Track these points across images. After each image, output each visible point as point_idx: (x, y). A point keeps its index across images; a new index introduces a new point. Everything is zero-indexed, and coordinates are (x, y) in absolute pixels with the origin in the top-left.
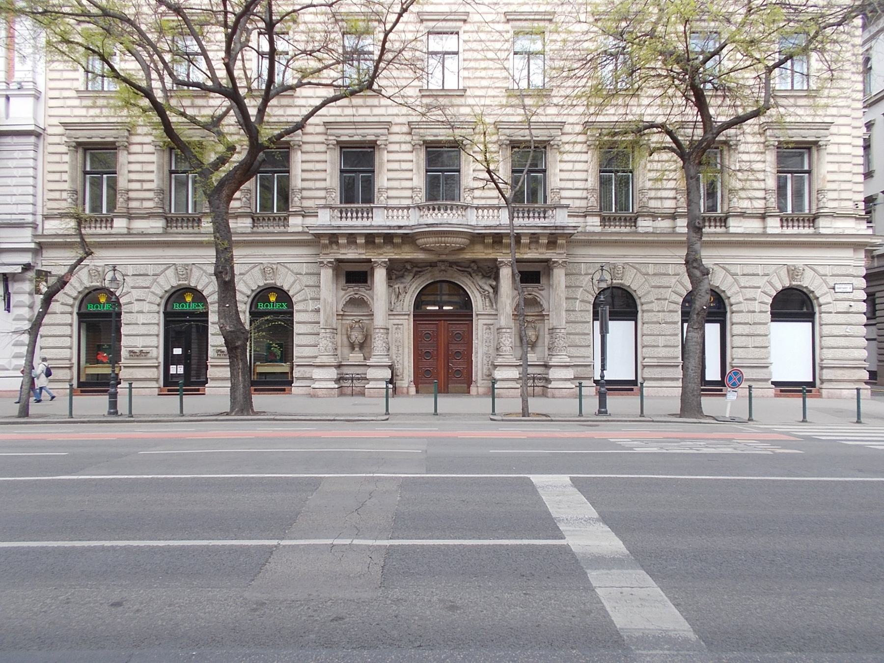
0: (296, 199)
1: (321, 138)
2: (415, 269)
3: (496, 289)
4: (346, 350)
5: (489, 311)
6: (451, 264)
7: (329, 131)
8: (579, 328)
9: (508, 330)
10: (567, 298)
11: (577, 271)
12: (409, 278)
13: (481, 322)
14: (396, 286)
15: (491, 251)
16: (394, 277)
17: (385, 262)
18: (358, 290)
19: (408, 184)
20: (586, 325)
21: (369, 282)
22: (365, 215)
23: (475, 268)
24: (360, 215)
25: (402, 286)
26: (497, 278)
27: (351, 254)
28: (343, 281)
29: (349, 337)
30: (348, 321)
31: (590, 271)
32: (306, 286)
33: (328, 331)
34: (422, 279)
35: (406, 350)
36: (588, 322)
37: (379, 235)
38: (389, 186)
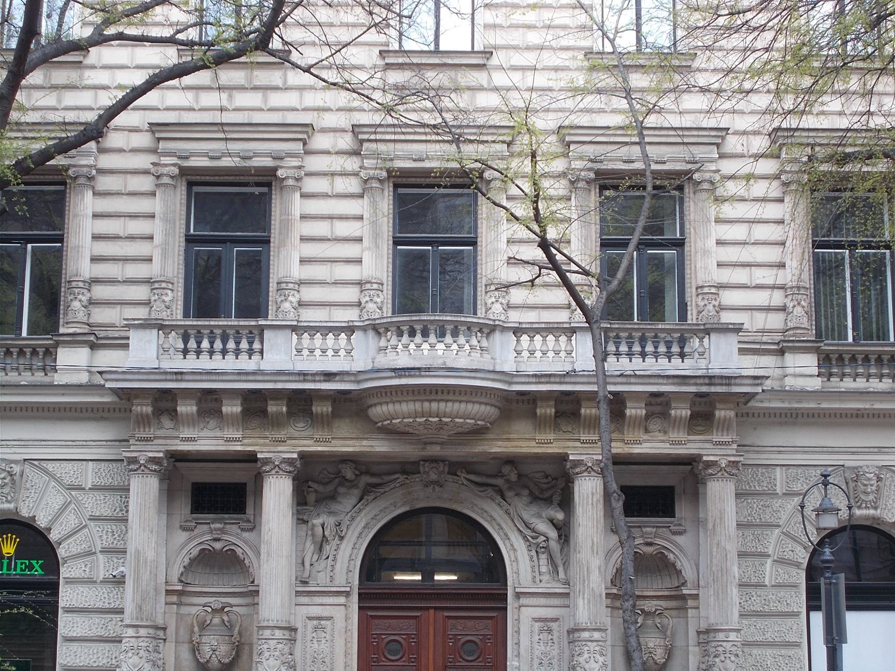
0: (76, 304)
1: (144, 161)
2: (366, 479)
3: (564, 531)
5: (548, 585)
6: (455, 467)
7: (162, 145)
8: (773, 630)
9: (597, 635)
10: (742, 555)
11: (764, 487)
12: (347, 503)
13: (528, 613)
14: (317, 521)
15: (551, 436)
16: (312, 498)
17: (290, 462)
18: (222, 531)
19: (351, 272)
20: (790, 622)
21: (250, 510)
22: (244, 345)
23: (513, 477)
24: (231, 345)
25: (330, 521)
26: (566, 502)
27: (207, 440)
28: (184, 508)
29: (195, 649)
30: (194, 609)
31: (798, 487)
32: (93, 519)
33: (143, 632)
34: (382, 503)
36: (796, 615)
37: (276, 395)
38: (304, 277)
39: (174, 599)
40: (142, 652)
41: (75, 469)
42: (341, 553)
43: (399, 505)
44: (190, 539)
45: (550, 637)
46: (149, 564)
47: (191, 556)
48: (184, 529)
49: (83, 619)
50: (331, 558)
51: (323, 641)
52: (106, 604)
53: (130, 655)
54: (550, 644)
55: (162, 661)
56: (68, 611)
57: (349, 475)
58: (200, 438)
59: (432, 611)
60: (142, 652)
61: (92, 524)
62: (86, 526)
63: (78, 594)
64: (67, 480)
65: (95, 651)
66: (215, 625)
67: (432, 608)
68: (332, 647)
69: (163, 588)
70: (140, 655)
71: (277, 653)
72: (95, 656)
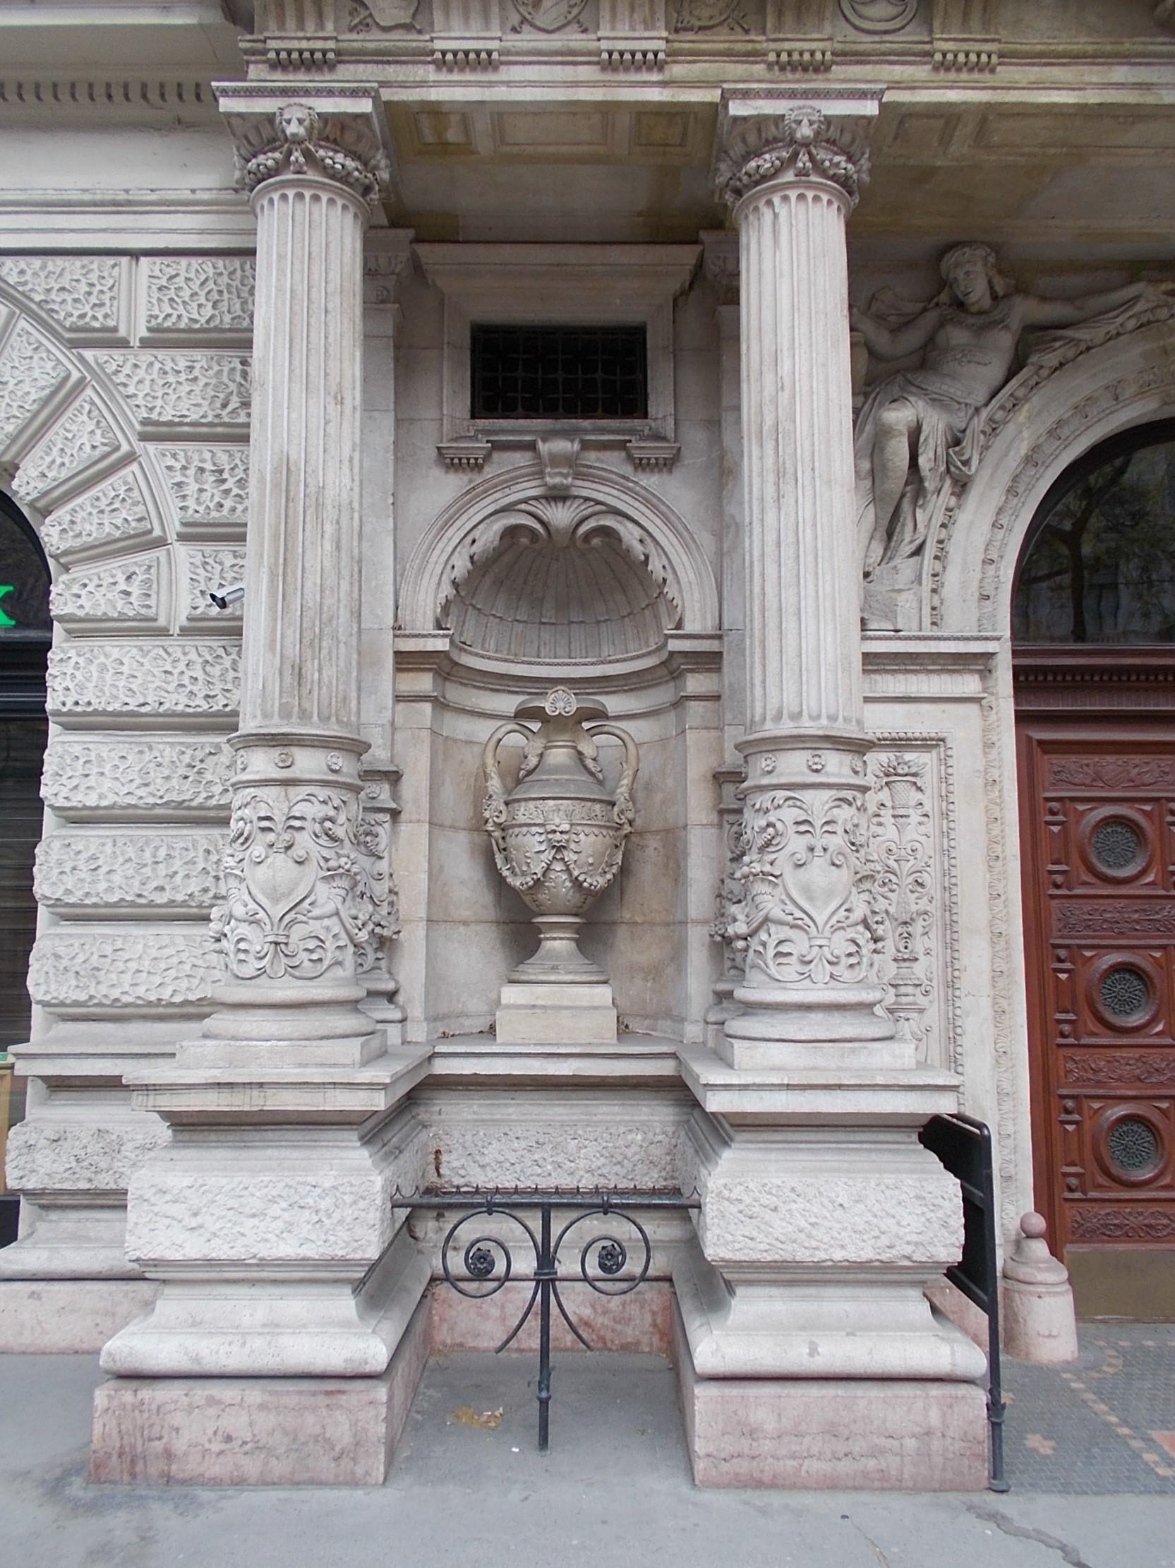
2: (1024, 310)
4: (473, 953)
28: (448, 395)
29: (492, 850)
32: (157, 432)
33: (308, 763)
34: (1083, 382)
35: (977, 958)
39: (424, 682)
40: (304, 842)
41: (93, 278)
42: (958, 532)
43: (1129, 392)
44: (471, 496)
46: (330, 513)
47: (475, 548)
48: (451, 462)
49: (122, 750)
50: (930, 550)
51: (915, 817)
52: (199, 701)
53: (258, 850)
55: (386, 884)
56: (81, 723)
58: (510, 57)
60: (304, 842)
61: (151, 447)
62: (131, 458)
63: (103, 668)
64: (68, 312)
65: (162, 853)
66: (557, 769)
68: (947, 834)
69: (387, 646)
70: (298, 852)
71: (837, 842)
72: (162, 870)
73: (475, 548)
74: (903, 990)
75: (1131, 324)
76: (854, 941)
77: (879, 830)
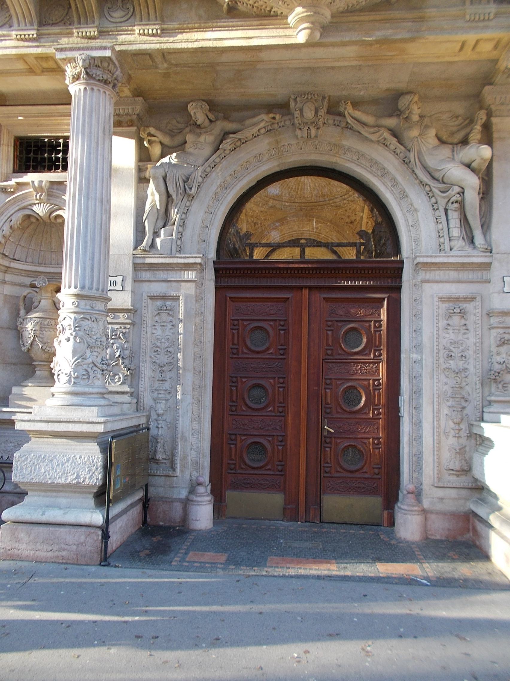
2: (222, 125)
5: (460, 253)
13: (432, 291)
45: (463, 322)
47: (12, 223)
54: (463, 331)
57: (200, 118)
59: (306, 292)
67: (306, 287)
73: (12, 223)
74: (160, 392)
75: (263, 131)
76: (86, 370)
77: (154, 331)
